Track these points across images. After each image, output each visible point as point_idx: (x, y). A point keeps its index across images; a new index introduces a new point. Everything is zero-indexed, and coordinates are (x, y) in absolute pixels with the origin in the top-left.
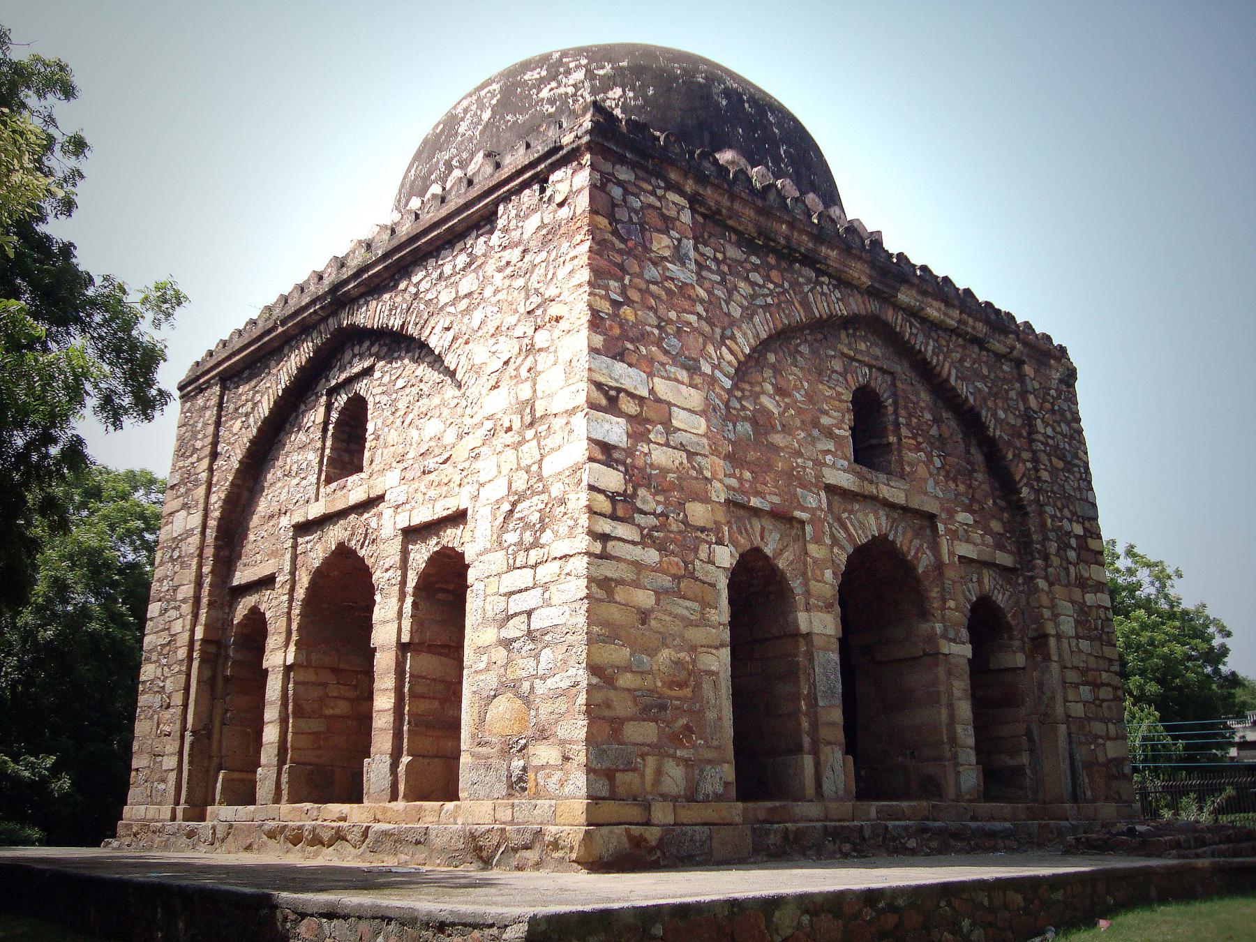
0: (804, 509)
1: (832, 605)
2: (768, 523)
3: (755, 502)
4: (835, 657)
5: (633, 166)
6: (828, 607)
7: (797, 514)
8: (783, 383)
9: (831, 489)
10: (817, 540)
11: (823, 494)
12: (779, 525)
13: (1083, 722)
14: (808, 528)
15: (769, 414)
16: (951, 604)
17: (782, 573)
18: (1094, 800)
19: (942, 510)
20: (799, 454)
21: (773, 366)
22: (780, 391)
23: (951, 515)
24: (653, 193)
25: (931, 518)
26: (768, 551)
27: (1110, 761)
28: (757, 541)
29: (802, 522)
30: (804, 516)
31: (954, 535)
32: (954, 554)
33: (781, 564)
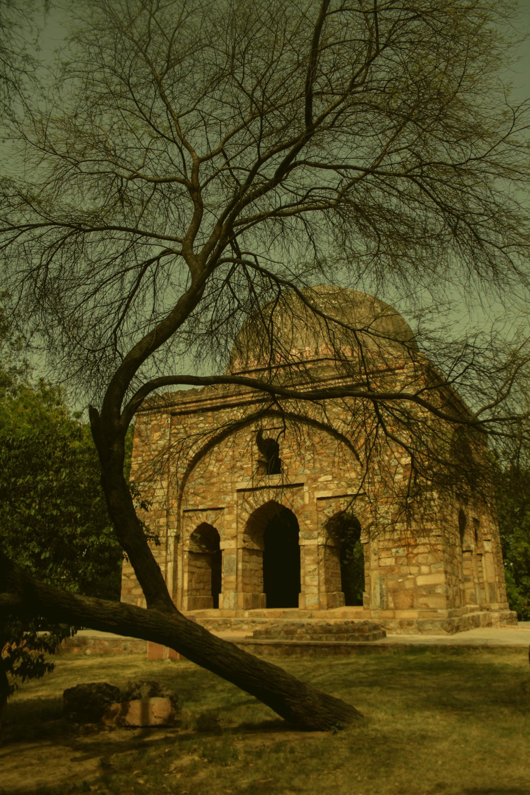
0: (223, 503)
1: (236, 537)
2: (209, 512)
3: (201, 507)
4: (234, 556)
5: (147, 415)
6: (235, 537)
7: (220, 506)
8: (220, 457)
9: (239, 491)
10: (230, 513)
11: (235, 495)
12: (215, 512)
13: (391, 569)
14: (226, 510)
15: (212, 472)
16: (308, 522)
17: (215, 529)
18: (396, 608)
19: (308, 480)
20: (225, 482)
21: (217, 452)
22: (218, 461)
23: (315, 480)
24: (156, 419)
25: (302, 485)
26: (209, 522)
27: (421, 587)
28: (203, 520)
29: (223, 508)
30: (223, 506)
31: (317, 489)
32: (313, 498)
33: (215, 526)
